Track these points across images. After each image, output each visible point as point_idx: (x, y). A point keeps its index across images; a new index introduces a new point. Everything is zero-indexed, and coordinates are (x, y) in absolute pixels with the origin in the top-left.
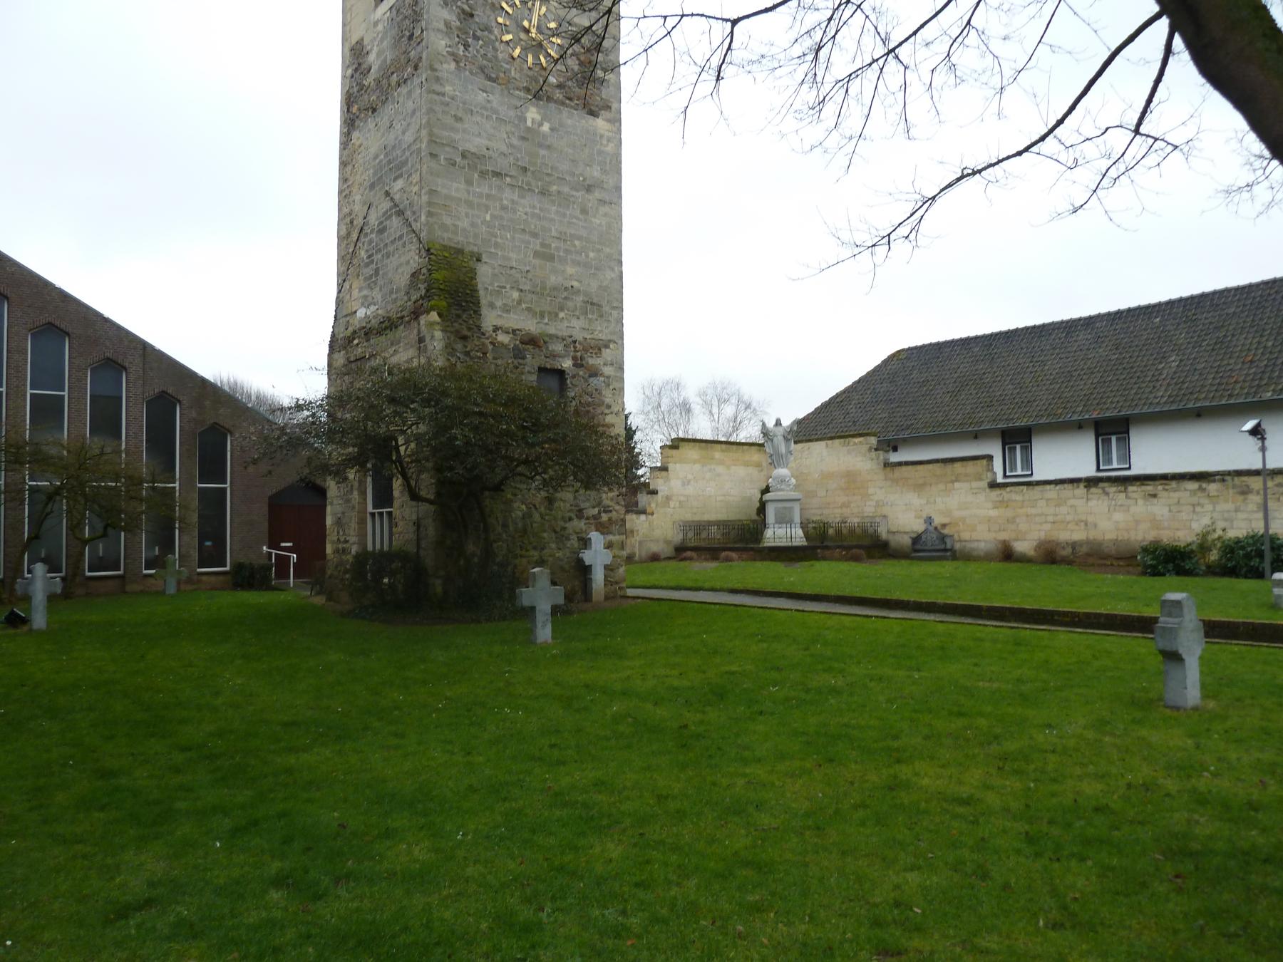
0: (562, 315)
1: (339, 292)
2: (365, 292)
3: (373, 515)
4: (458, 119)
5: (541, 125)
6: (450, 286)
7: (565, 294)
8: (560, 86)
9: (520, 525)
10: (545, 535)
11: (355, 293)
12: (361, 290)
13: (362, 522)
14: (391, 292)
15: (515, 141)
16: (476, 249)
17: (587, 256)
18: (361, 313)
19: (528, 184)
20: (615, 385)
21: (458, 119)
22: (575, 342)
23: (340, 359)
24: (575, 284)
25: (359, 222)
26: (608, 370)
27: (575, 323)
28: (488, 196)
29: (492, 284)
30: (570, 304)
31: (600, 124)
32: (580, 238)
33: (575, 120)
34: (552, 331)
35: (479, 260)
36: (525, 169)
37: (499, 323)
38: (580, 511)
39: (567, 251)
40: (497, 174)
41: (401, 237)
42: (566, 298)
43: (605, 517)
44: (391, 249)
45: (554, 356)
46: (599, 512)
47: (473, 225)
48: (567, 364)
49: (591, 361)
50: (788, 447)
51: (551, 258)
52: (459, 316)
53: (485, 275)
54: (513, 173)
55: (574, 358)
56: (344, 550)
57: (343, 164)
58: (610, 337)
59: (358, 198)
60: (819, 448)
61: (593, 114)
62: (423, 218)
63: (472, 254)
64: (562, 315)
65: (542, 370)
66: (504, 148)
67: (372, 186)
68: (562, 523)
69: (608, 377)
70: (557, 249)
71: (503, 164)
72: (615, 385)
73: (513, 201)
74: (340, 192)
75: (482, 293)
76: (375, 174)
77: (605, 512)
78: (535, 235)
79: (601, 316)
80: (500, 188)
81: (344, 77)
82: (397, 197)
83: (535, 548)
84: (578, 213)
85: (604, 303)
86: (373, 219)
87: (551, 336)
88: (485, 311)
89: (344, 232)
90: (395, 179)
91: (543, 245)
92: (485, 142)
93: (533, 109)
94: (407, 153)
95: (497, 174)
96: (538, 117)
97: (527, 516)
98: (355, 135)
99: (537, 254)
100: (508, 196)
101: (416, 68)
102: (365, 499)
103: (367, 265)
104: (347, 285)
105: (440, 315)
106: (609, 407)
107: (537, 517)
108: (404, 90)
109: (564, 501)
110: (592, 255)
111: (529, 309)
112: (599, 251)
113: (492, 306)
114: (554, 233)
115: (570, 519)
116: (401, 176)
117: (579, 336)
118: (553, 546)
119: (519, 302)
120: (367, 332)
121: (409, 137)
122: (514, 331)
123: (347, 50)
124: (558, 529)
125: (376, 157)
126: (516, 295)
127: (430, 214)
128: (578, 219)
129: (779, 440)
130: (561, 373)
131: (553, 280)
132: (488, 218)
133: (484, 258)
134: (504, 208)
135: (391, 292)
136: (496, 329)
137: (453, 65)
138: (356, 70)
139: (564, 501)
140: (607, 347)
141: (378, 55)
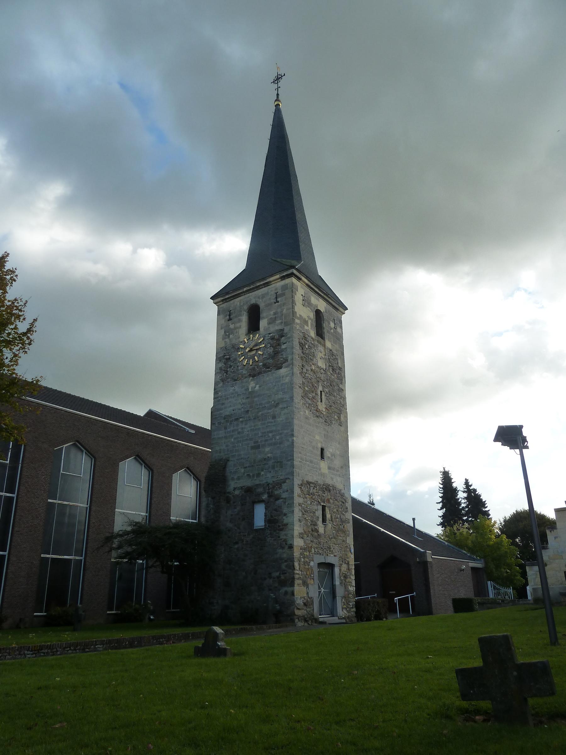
0: (262, 473)
4: (223, 404)
17: (275, 439)
21: (223, 404)
24: (269, 455)
27: (269, 475)
30: (267, 466)
31: (283, 371)
32: (271, 432)
34: (257, 482)
38: (270, 574)
39: (266, 440)
42: (265, 464)
46: (280, 574)
47: (227, 446)
49: (276, 492)
51: (258, 447)
54: (243, 416)
55: (268, 493)
64: (262, 473)
69: (285, 499)
70: (261, 441)
73: (242, 429)
77: (283, 574)
78: (251, 439)
79: (282, 467)
80: (237, 425)
84: (271, 420)
87: (257, 485)
91: (255, 442)
92: (231, 408)
99: (253, 448)
111: (247, 475)
112: (281, 434)
114: (260, 434)
115: (265, 579)
117: (270, 481)
122: (242, 487)
126: (243, 470)
128: (272, 422)
131: (260, 457)
132: (232, 440)
133: (231, 459)
134: (239, 433)
140: (284, 482)
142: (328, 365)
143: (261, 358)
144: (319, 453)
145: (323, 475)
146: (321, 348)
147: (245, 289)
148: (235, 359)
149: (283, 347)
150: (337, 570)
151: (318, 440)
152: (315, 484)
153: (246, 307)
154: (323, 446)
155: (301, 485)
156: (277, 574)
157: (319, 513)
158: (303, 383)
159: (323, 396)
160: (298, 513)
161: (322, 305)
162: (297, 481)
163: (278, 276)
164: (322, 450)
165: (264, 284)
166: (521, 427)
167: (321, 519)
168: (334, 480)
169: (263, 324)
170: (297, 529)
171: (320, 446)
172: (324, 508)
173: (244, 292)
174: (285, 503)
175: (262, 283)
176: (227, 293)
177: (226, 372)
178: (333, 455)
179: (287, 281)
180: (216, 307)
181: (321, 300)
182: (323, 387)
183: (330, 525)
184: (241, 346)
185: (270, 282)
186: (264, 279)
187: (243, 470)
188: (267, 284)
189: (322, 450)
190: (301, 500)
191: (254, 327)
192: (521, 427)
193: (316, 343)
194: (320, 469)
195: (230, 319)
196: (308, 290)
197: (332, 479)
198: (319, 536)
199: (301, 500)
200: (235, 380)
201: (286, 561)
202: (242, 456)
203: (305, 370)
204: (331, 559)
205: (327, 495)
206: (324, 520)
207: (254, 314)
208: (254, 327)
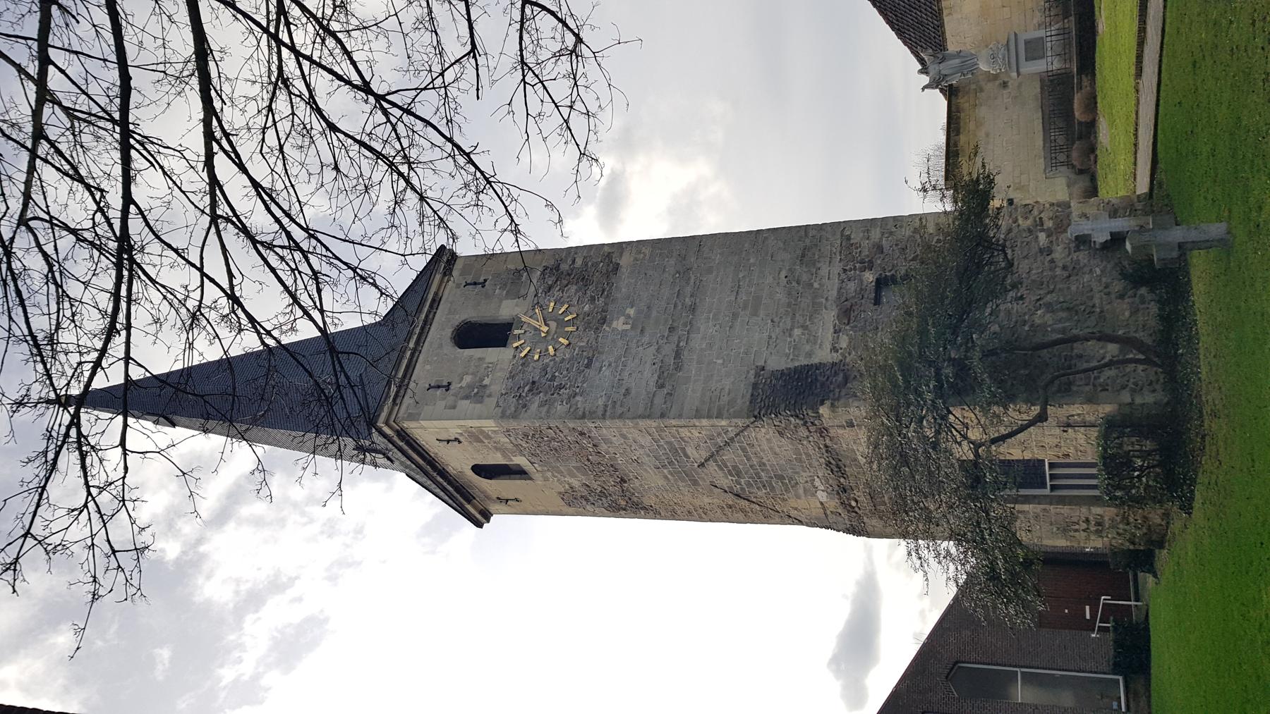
0: (816, 285)
1: (801, 523)
2: (801, 491)
3: (1053, 488)
4: (628, 391)
5: (629, 316)
6: (793, 393)
7: (794, 284)
8: (593, 299)
9: (1064, 315)
10: (1073, 288)
11: (801, 503)
12: (798, 497)
13: (1062, 501)
14: (800, 461)
15: (646, 339)
16: (752, 372)
17: (754, 265)
18: (822, 496)
19: (685, 325)
20: (890, 226)
21: (628, 391)
22: (845, 270)
23: (873, 523)
25: (730, 499)
26: (876, 234)
27: (824, 271)
28: (699, 362)
29: (788, 356)
30: (805, 278)
31: (625, 260)
33: (624, 283)
35: (763, 369)
36: (672, 329)
37: (828, 346)
38: (1041, 251)
40: (678, 354)
41: (744, 450)
43: (1049, 224)
44: (755, 461)
45: (861, 291)
48: (870, 277)
50: (953, 57)
52: (823, 385)
53: (777, 362)
54: (676, 339)
55: (863, 270)
56: (1098, 524)
57: (674, 516)
58: (838, 236)
59: (707, 500)
60: (952, 26)
61: (617, 267)
62: (724, 423)
63: (757, 375)
65: (877, 301)
66: (653, 349)
67: (695, 483)
68: (1058, 271)
69: (883, 234)
71: (669, 349)
72: (890, 226)
73: (704, 338)
74: (701, 519)
75: (797, 364)
76: (683, 480)
81: (594, 515)
82: (705, 454)
83: (1091, 298)
85: (801, 245)
86: (725, 482)
88: (815, 361)
89: (741, 515)
90: (687, 456)
91: (745, 308)
93: (614, 324)
94: (662, 442)
95: (678, 354)
96: (622, 319)
97: (1049, 307)
98: (647, 501)
99: (755, 313)
100: (697, 342)
101: (582, 434)
102: (1035, 497)
103: (773, 489)
104: (793, 513)
105: (822, 403)
106: (916, 231)
107: (1049, 298)
108: (603, 447)
109: (1031, 270)
110: (752, 261)
113: (809, 355)
115: (1052, 261)
116: (683, 450)
117: (837, 268)
118: (1086, 278)
119: (804, 327)
120: (842, 491)
121: (646, 441)
123: (571, 510)
124: (1066, 274)
125: (666, 477)
126: (797, 332)
127: (719, 416)
129: (945, 68)
130: (881, 284)
131: (781, 296)
132: (720, 361)
133: (761, 363)
134: (710, 346)
135: (800, 461)
136: (834, 349)
137: (578, 398)
138: (587, 500)
139: (1031, 270)
140: (849, 238)
141: (573, 476)
156: (1042, 236)
165: (431, 306)
173: (414, 350)
174: (891, 233)
175: (426, 309)
185: (436, 294)
188: (436, 302)
201: (1016, 221)
202: (766, 335)
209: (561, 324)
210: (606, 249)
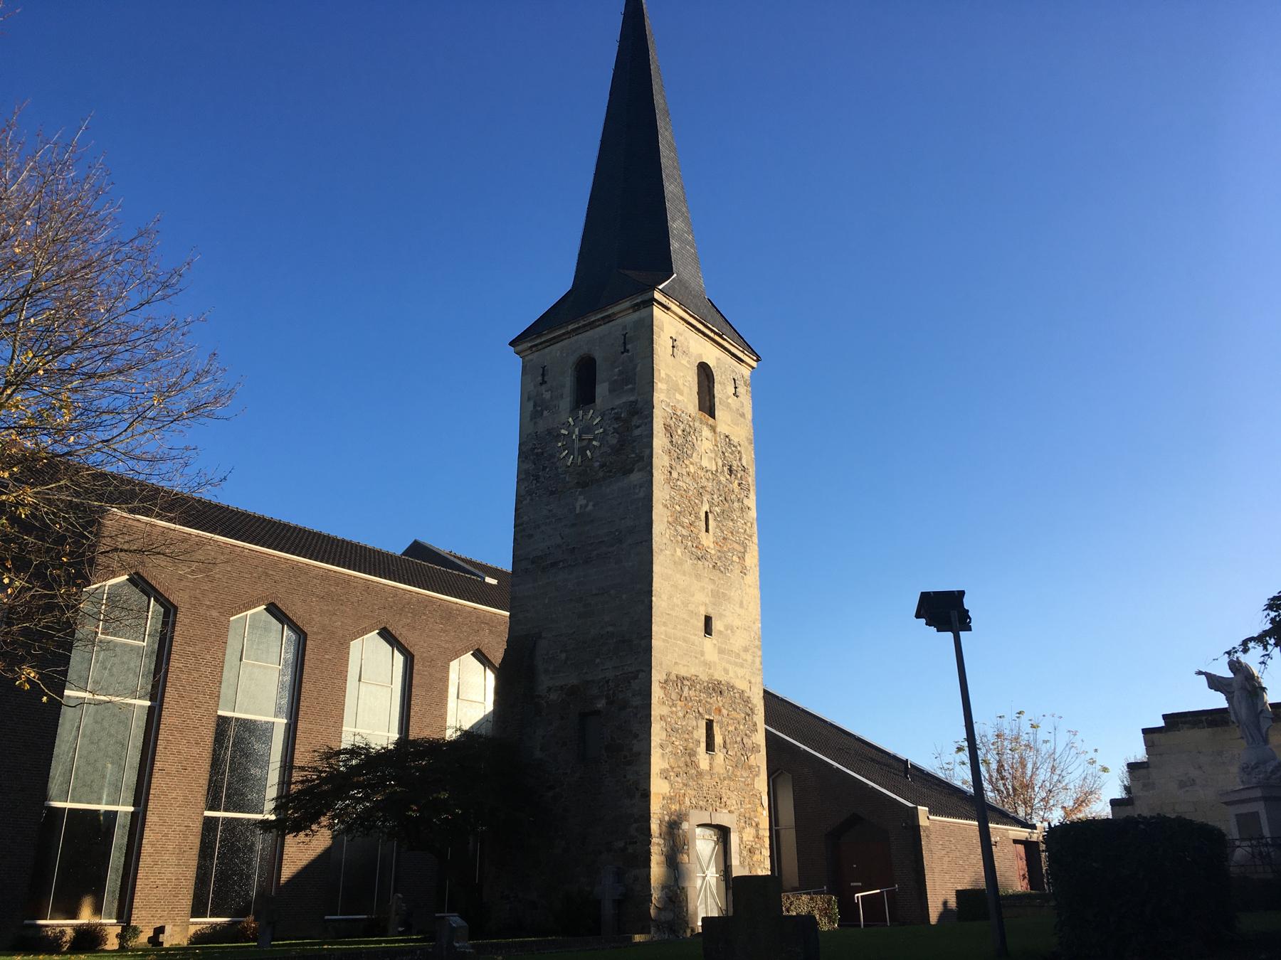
4: (530, 536)
21: (530, 536)
26: (636, 701)
31: (635, 477)
40: (554, 565)
48: (601, 704)
95: (554, 565)
96: (584, 502)
126: (563, 656)
140: (636, 677)
142: (720, 464)
143: (597, 453)
144: (702, 624)
145: (708, 665)
146: (706, 432)
147: (570, 327)
148: (552, 456)
149: (637, 432)
150: (734, 838)
151: (701, 603)
152: (693, 682)
153: (572, 359)
154: (712, 613)
155: (666, 681)
156: (621, 844)
157: (701, 734)
158: (672, 498)
159: (711, 522)
160: (658, 733)
161: (712, 355)
162: (657, 676)
163: (626, 304)
164: (708, 620)
165: (603, 318)
166: (962, 593)
167: (703, 745)
168: (731, 674)
169: (601, 390)
170: (658, 762)
171: (703, 612)
172: (709, 725)
173: (568, 333)
175: (599, 316)
176: (540, 335)
177: (537, 478)
178: (727, 627)
179: (643, 313)
180: (518, 361)
181: (709, 345)
182: (711, 504)
183: (720, 755)
184: (563, 431)
185: (614, 314)
186: (602, 309)
187: (563, 656)
188: (609, 319)
189: (708, 620)
190: (665, 710)
191: (585, 395)
192: (962, 593)
193: (697, 424)
194: (702, 654)
195: (543, 382)
196: (682, 327)
197: (726, 671)
198: (700, 774)
199: (665, 710)
200: (552, 493)
203: (675, 475)
204: (723, 818)
205: (717, 701)
206: (710, 747)
207: (586, 371)
208: (585, 395)
209: (582, 451)
210: (647, 451)
